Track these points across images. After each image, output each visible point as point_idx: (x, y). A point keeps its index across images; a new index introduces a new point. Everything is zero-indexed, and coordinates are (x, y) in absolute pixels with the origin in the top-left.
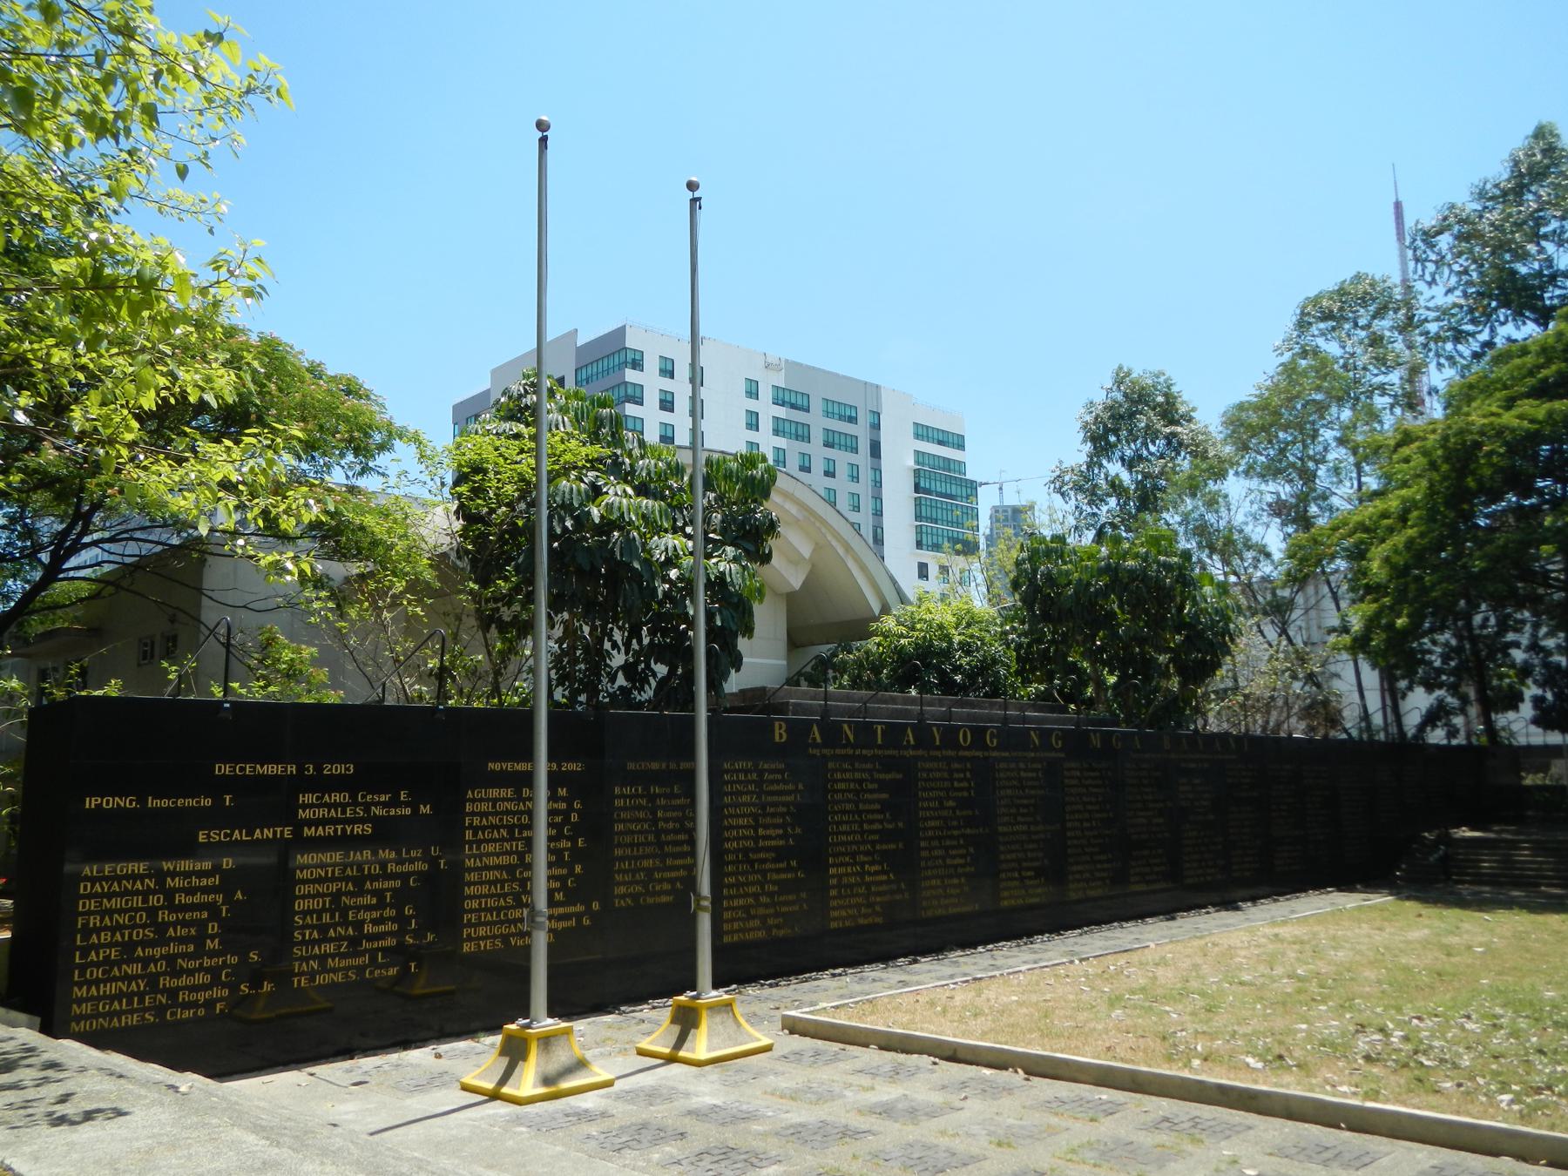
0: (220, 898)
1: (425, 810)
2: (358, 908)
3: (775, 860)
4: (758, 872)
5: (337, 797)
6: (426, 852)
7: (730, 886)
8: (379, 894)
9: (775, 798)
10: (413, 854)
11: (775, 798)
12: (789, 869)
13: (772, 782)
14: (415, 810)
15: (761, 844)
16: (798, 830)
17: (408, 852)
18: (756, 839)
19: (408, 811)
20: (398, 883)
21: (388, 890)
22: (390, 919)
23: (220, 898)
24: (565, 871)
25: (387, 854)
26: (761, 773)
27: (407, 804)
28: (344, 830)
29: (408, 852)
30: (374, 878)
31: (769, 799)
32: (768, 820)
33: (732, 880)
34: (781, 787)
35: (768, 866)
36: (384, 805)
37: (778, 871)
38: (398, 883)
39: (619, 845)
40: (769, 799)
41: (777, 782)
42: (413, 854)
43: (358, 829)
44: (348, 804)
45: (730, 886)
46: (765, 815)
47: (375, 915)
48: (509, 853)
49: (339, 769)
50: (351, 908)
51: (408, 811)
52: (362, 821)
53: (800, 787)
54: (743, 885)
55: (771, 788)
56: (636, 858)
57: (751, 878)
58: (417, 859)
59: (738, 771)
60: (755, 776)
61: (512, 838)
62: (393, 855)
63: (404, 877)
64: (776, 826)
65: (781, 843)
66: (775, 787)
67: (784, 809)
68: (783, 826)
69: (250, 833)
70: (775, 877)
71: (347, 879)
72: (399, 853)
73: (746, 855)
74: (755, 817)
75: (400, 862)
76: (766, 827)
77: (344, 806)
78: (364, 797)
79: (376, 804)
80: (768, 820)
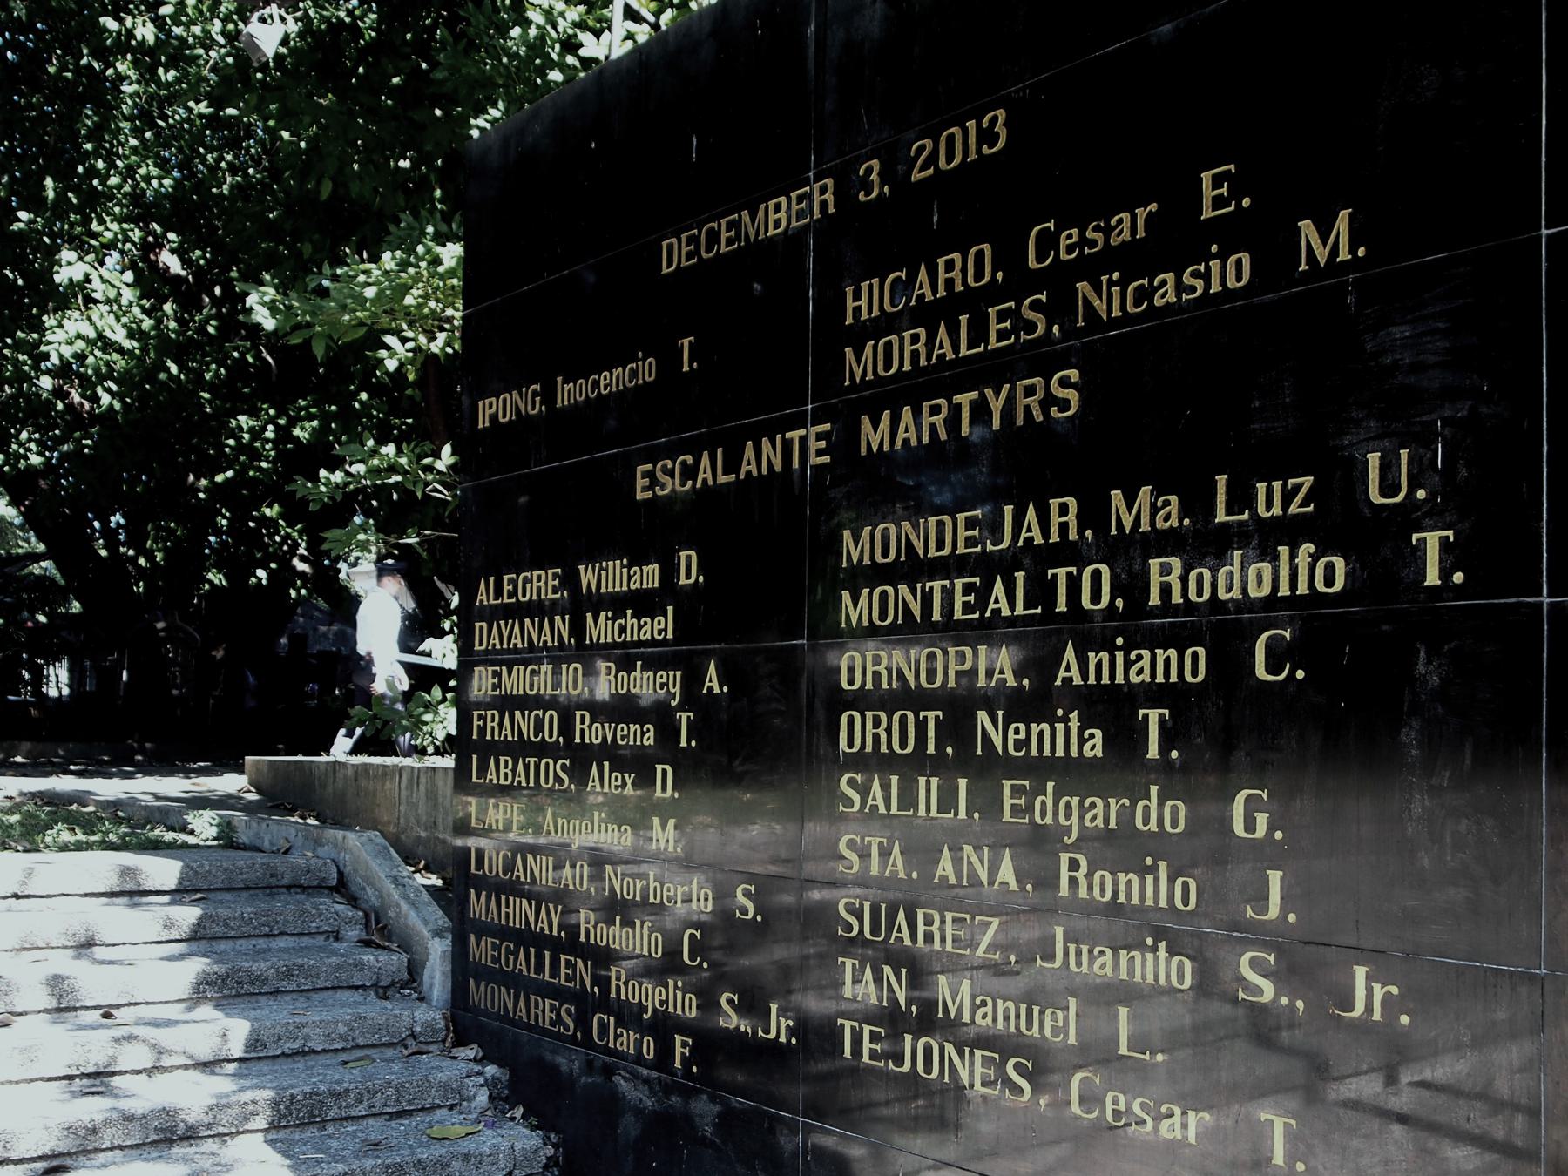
0: (673, 681)
1: (1329, 241)
2: (1038, 769)
5: (956, 270)
6: (1340, 483)
8: (1112, 709)
10: (1268, 500)
14: (1275, 254)
17: (1241, 498)
19: (1232, 272)
20: (1194, 665)
21: (1155, 694)
22: (1158, 843)
23: (673, 681)
25: (1134, 510)
27: (1230, 235)
28: (980, 411)
29: (1241, 498)
30: (1089, 633)
36: (1133, 261)
38: (1194, 665)
42: (1268, 500)
43: (1023, 398)
44: (993, 293)
47: (1103, 812)
49: (961, 144)
50: (1012, 767)
51: (1232, 272)
52: (1042, 360)
58: (1288, 531)
62: (1171, 514)
63: (1225, 629)
69: (732, 465)
72: (1197, 503)
75: (1204, 544)
77: (974, 302)
78: (1047, 243)
79: (1090, 268)
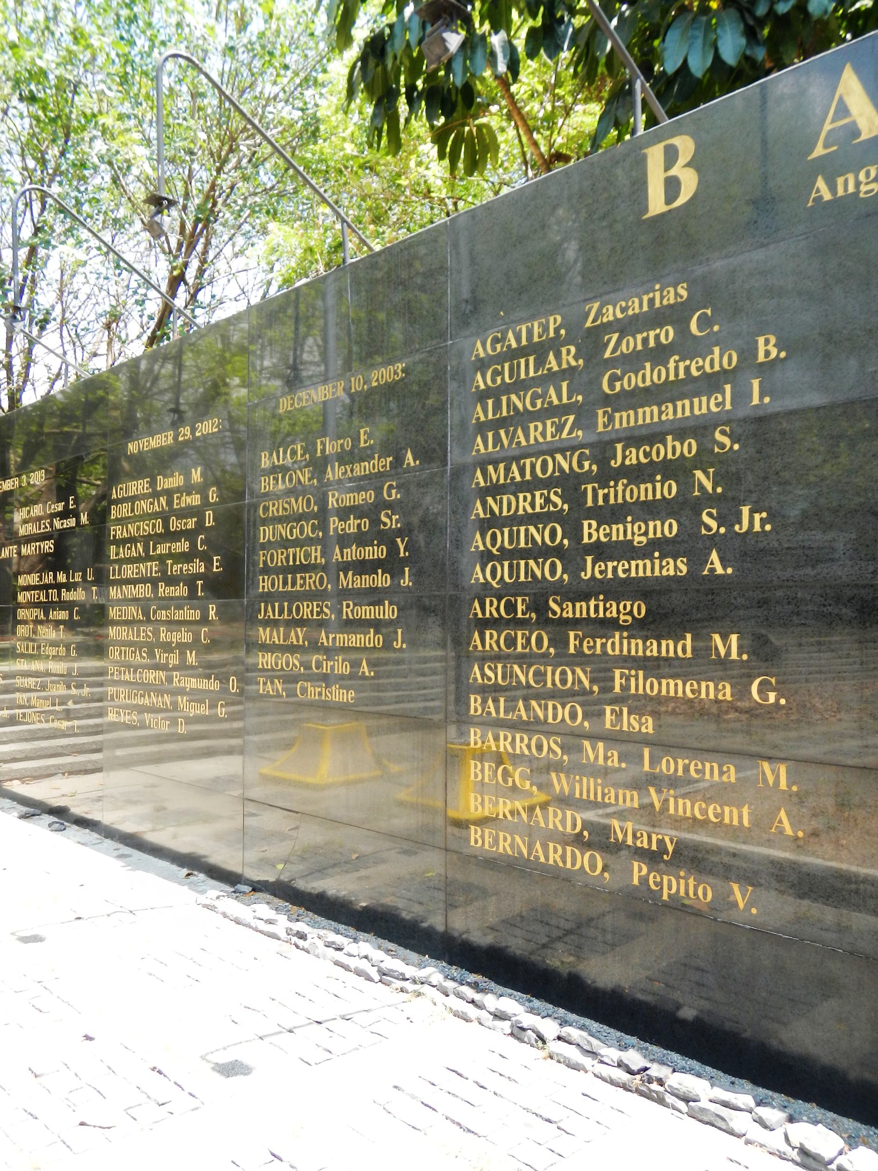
3: (643, 627)
4: (580, 659)
7: (491, 691)
9: (648, 415)
11: (648, 415)
12: (704, 665)
13: (633, 362)
15: (591, 570)
16: (751, 520)
18: (572, 556)
24: (196, 615)
26: (592, 342)
31: (624, 420)
32: (621, 492)
33: (494, 674)
34: (675, 368)
35: (617, 645)
37: (654, 667)
39: (266, 570)
40: (624, 420)
41: (659, 355)
45: (491, 691)
46: (606, 476)
48: (143, 580)
53: (767, 348)
54: (529, 695)
55: (632, 381)
56: (292, 597)
57: (552, 677)
59: (512, 355)
60: (569, 357)
61: (148, 558)
64: (650, 510)
65: (675, 567)
66: (650, 375)
67: (689, 448)
68: (685, 507)
70: (642, 684)
71: (37, 605)
73: (539, 606)
74: (570, 485)
76: (611, 514)
80: (621, 492)
